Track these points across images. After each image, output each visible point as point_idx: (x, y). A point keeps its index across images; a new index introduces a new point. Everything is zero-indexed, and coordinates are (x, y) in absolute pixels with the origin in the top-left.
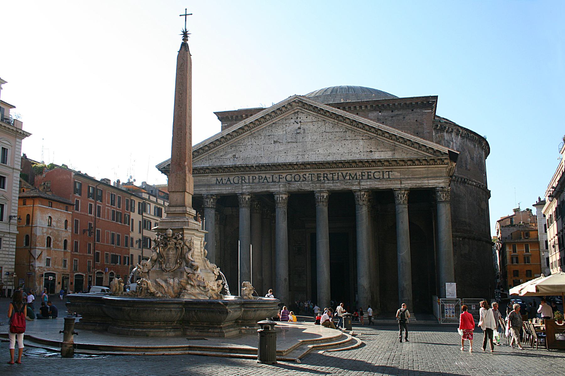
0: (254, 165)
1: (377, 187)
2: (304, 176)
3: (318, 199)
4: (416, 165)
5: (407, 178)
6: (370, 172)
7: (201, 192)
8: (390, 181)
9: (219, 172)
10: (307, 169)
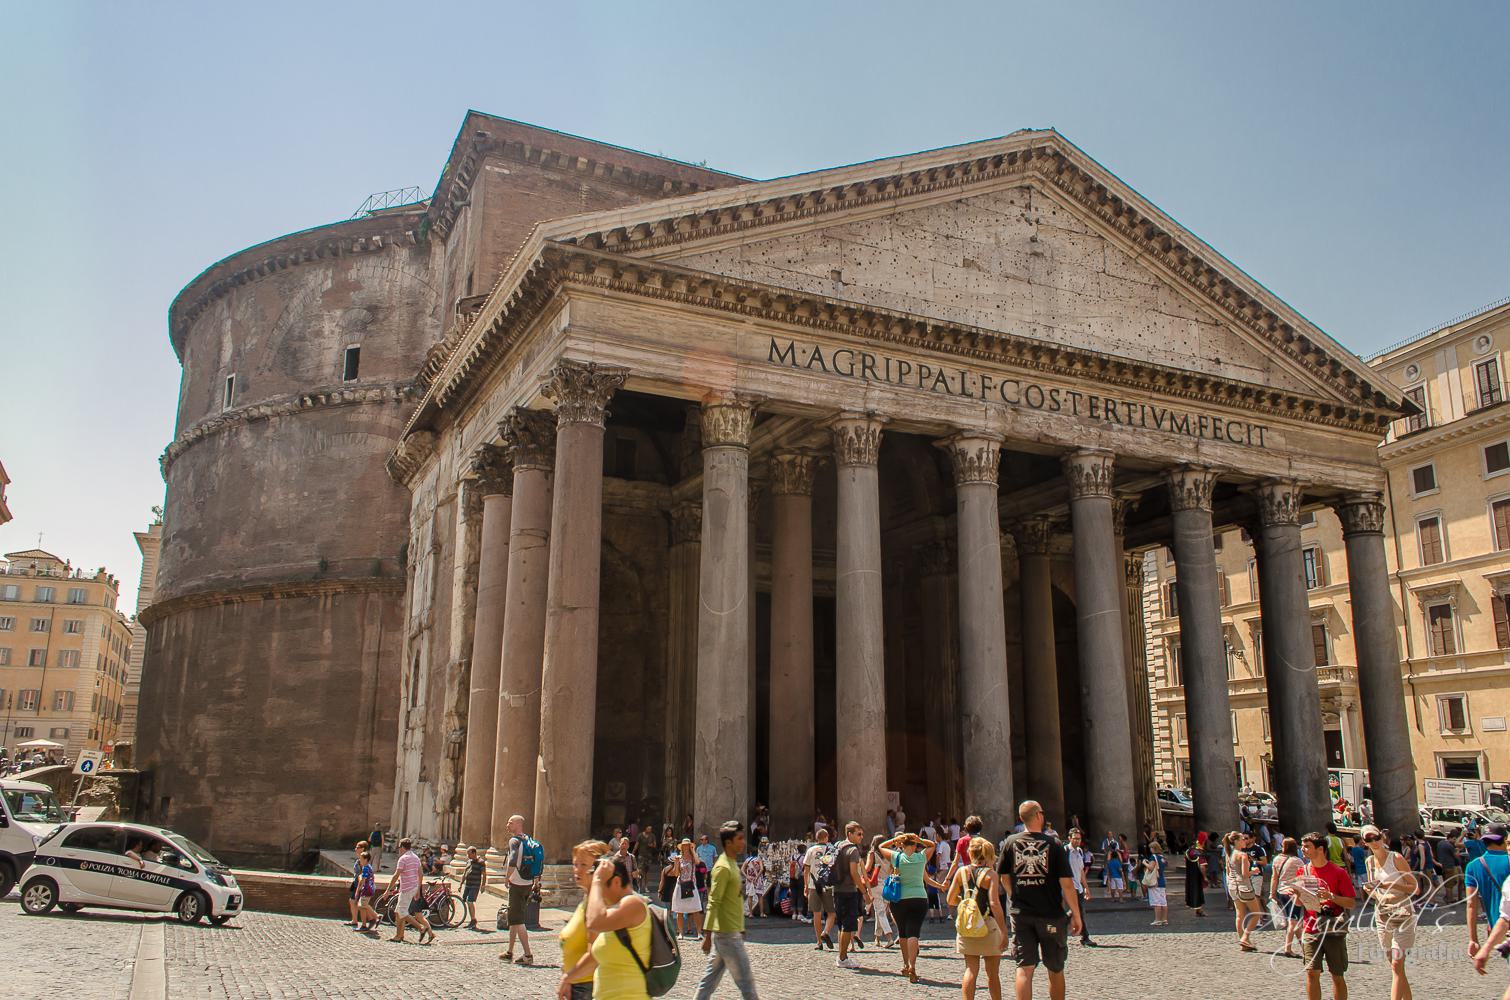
0: (932, 322)
2: (1054, 394)
3: (1096, 476)
4: (1323, 423)
5: (1305, 456)
6: (1220, 420)
7: (709, 379)
10: (1069, 374)
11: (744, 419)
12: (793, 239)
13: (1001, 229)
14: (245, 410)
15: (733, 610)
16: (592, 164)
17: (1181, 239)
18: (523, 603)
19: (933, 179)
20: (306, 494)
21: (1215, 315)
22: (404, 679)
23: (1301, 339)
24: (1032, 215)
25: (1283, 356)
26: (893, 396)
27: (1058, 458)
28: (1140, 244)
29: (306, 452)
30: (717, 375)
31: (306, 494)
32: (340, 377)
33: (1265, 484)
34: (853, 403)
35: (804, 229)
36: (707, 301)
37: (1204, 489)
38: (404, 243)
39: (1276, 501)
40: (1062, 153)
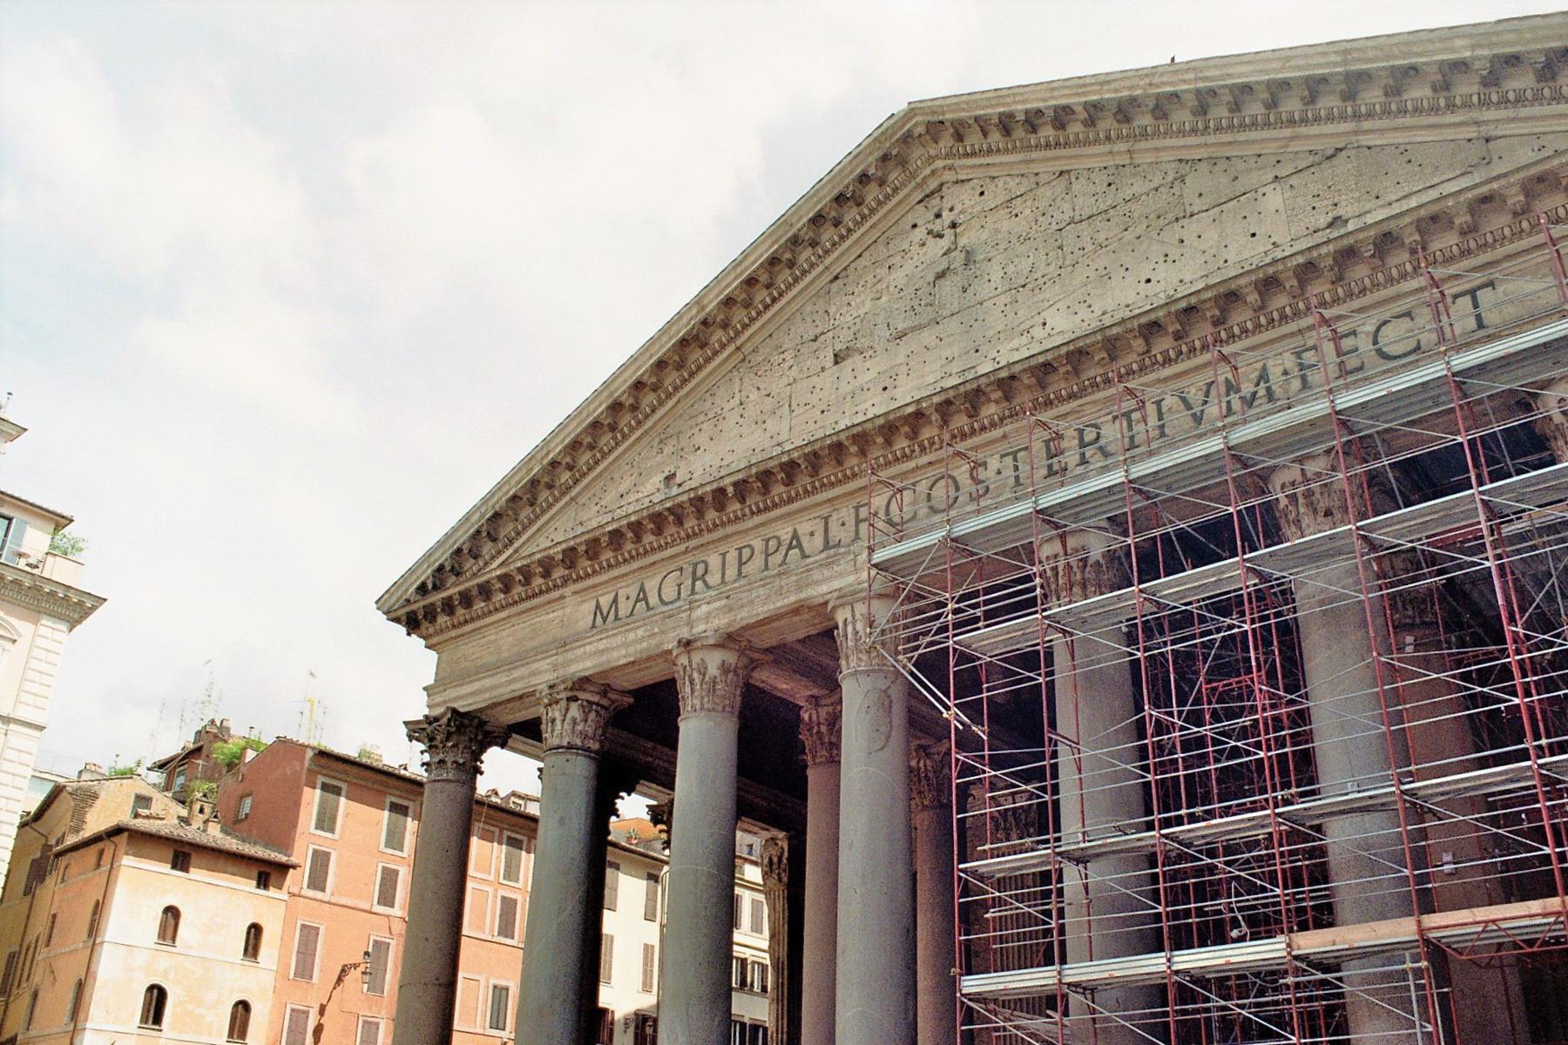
0: (728, 481)
6: (1354, 333)
7: (534, 681)
10: (983, 429)
12: (627, 467)
13: (892, 278)
17: (1157, 86)
25: (1510, 113)
26: (723, 602)
30: (540, 673)
40: (935, 118)
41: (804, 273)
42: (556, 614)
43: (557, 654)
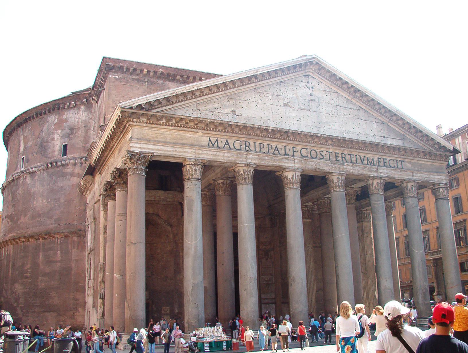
0: (271, 128)
1: (393, 176)
2: (321, 152)
3: (339, 183)
4: (424, 158)
5: (418, 171)
6: (386, 159)
7: (185, 154)
8: (404, 171)
9: (216, 130)
10: (326, 145)
11: (199, 169)
13: (298, 91)
14: (28, 169)
15: (196, 241)
16: (149, 72)
17: (367, 93)
18: (120, 241)
19: (270, 75)
20: (50, 200)
21: (383, 120)
22: (86, 269)
23: (414, 127)
24: (310, 85)
26: (257, 157)
27: (324, 177)
28: (352, 95)
29: (49, 184)
30: (188, 153)
31: (50, 200)
32: (61, 156)
33: (405, 182)
34: (242, 160)
35: (220, 96)
36: (183, 126)
37: (380, 186)
38: (82, 103)
39: (408, 189)
40: (319, 63)
41: (277, 77)
42: (191, 135)
43: (195, 149)
